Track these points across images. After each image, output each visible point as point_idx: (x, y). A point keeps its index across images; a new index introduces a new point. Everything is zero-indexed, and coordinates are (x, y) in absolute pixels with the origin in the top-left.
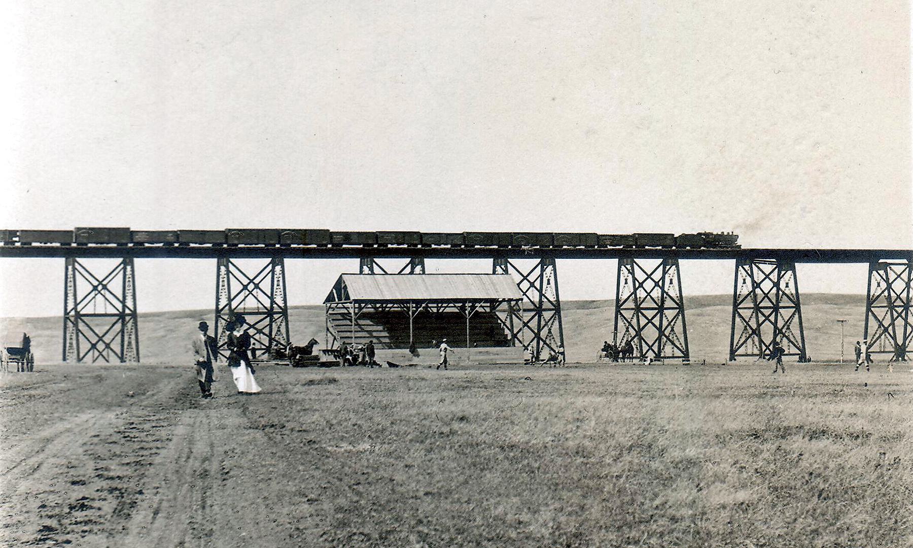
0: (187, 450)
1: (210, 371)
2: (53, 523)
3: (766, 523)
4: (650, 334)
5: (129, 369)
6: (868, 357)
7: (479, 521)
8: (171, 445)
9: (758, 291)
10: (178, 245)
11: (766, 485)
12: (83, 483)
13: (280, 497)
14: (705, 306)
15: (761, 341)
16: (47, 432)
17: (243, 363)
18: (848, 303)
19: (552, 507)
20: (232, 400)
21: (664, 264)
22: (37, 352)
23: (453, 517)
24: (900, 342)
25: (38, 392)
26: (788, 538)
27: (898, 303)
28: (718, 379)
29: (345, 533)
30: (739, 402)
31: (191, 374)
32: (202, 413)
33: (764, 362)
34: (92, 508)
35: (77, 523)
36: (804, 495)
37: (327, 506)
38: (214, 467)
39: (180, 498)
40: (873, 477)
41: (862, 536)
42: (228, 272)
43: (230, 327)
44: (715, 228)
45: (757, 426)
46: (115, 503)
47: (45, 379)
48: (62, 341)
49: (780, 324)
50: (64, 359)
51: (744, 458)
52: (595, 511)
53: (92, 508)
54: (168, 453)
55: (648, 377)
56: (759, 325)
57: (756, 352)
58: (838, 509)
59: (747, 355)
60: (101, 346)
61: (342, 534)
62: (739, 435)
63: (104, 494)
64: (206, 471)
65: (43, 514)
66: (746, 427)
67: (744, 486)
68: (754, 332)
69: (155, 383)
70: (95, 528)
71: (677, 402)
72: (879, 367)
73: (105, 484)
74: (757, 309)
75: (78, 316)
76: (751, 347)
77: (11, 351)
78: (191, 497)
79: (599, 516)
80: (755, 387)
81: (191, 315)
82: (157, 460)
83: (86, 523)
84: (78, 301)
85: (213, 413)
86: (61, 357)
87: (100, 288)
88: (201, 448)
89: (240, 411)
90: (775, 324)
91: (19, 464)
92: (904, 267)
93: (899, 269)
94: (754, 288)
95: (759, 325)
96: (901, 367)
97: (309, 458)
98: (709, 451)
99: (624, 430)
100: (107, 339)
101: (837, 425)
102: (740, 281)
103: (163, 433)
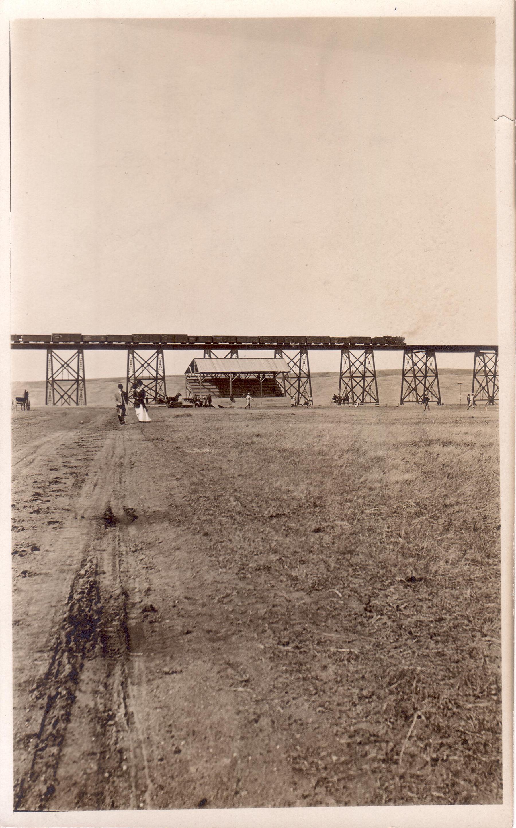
0: (111, 452)
1: (124, 410)
2: (40, 491)
3: (420, 491)
4: (358, 390)
5: (81, 409)
6: (474, 402)
7: (267, 490)
8: (103, 449)
9: (415, 367)
10: (107, 343)
11: (420, 471)
12: (57, 470)
13: (161, 477)
14: (387, 375)
15: (417, 394)
16: (37, 443)
17: (141, 405)
18: (463, 374)
19: (306, 483)
20: (136, 426)
21: (366, 353)
22: (31, 400)
23: (253, 488)
24: (491, 395)
25: (32, 421)
26: (431, 499)
27: (490, 374)
28: (394, 414)
29: (195, 496)
30: (405, 426)
31: (114, 412)
32: (120, 433)
33: (419, 405)
34: (61, 483)
35: (53, 491)
36: (440, 476)
37: (186, 482)
38: (126, 461)
39: (108, 478)
40: (477, 467)
41: (471, 498)
42: (134, 357)
43: (135, 386)
44: (392, 334)
45: (415, 440)
46: (73, 480)
47: (36, 414)
48: (45, 394)
49: (427, 385)
50: (46, 404)
51: (408, 457)
52: (329, 484)
53: (61, 483)
54: (101, 454)
55: (357, 413)
56: (416, 386)
57: (415, 400)
58: (458, 483)
59: (410, 401)
60: (66, 397)
61: (194, 497)
62: (406, 444)
63: (68, 476)
64: (122, 463)
65: (35, 486)
66: (409, 440)
67: (408, 471)
68: (413, 389)
69: (95, 416)
70: (63, 494)
71: (373, 427)
72: (480, 408)
73: (68, 470)
74: (415, 377)
75: (54, 380)
76: (412, 397)
77: (18, 399)
78: (114, 477)
79: (331, 487)
80: (414, 418)
81: (114, 380)
82: (96, 457)
83: (58, 491)
84: (54, 372)
85: (125, 432)
86: (45, 402)
87: (65, 366)
88: (119, 451)
89: (140, 431)
90: (425, 385)
91: (22, 459)
92: (493, 355)
93: (491, 356)
94: (413, 366)
95: (416, 386)
96: (492, 408)
97: (177, 456)
98: (390, 453)
99: (344, 442)
100: (69, 393)
101: (457, 439)
102: (406, 362)
103: (99, 443)
